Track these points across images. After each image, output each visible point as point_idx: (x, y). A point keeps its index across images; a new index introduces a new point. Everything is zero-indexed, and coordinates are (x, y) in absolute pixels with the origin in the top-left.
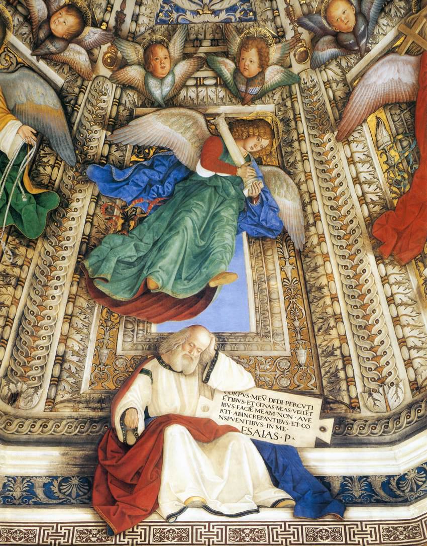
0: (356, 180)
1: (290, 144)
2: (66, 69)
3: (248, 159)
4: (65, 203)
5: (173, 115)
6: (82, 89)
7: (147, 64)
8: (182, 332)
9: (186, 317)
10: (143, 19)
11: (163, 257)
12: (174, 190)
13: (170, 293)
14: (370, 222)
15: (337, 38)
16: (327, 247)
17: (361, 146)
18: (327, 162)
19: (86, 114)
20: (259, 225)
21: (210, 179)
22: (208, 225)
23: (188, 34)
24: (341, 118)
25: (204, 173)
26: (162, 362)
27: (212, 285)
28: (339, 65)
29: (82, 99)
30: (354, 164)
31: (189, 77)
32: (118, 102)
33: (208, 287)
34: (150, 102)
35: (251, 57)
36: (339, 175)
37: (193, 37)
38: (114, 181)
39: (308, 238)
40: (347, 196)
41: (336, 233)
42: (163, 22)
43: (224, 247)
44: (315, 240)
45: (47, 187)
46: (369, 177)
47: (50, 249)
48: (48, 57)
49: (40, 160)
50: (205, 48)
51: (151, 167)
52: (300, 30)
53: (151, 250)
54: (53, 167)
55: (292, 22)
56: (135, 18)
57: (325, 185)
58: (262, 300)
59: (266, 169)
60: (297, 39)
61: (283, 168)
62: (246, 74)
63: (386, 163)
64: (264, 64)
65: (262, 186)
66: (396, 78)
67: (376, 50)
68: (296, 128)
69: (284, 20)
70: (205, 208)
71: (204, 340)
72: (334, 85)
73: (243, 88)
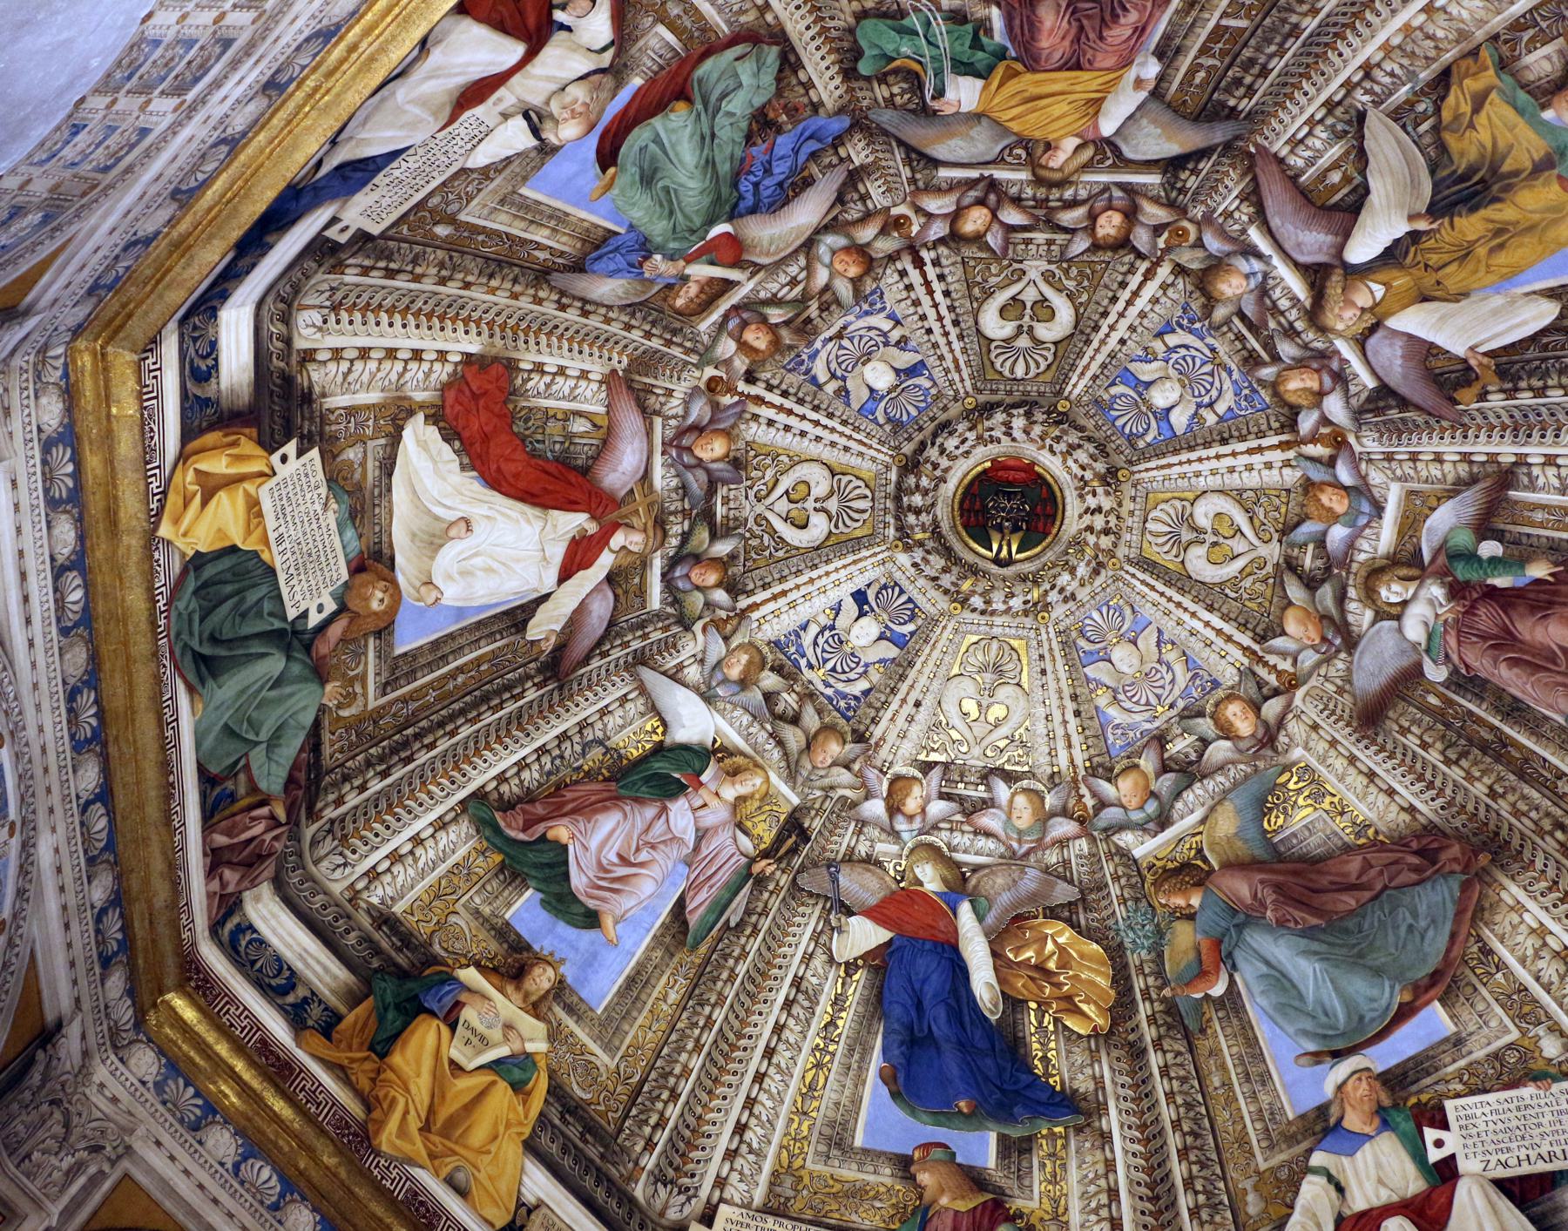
0: (561, 371)
1: (653, 324)
2: (944, 186)
3: (685, 279)
4: (849, 73)
5: (797, 238)
8: (602, 111)
9: (612, 122)
11: (692, 136)
12: (737, 190)
13: (652, 121)
14: (511, 366)
16: (525, 303)
17: (589, 394)
18: (601, 348)
19: (891, 163)
20: (617, 249)
21: (707, 232)
22: (670, 202)
24: (630, 388)
26: (595, 72)
27: (612, 170)
28: (674, 417)
29: (906, 172)
30: (578, 378)
31: (808, 277)
32: (864, 198)
33: (614, 164)
35: (757, 338)
36: (580, 352)
37: (833, 307)
38: (811, 137)
39: (552, 288)
40: (555, 351)
41: (529, 318)
42: (872, 294)
43: (634, 204)
44: (542, 294)
45: (886, 74)
46: (555, 388)
47: (831, 24)
48: (971, 184)
49: (914, 93)
50: (813, 310)
51: (780, 184)
52: (736, 398)
53: (712, 128)
54: (892, 95)
55: (748, 396)
56: (903, 274)
57: (583, 332)
58: (541, 213)
59: (656, 288)
60: (732, 390)
61: (641, 303)
62: (753, 327)
63: (554, 416)
64: (743, 346)
65: (647, 275)
66: (621, 469)
67: (658, 460)
68: (660, 337)
70: (688, 210)
71: (568, 131)
72: (662, 399)
73: (745, 315)
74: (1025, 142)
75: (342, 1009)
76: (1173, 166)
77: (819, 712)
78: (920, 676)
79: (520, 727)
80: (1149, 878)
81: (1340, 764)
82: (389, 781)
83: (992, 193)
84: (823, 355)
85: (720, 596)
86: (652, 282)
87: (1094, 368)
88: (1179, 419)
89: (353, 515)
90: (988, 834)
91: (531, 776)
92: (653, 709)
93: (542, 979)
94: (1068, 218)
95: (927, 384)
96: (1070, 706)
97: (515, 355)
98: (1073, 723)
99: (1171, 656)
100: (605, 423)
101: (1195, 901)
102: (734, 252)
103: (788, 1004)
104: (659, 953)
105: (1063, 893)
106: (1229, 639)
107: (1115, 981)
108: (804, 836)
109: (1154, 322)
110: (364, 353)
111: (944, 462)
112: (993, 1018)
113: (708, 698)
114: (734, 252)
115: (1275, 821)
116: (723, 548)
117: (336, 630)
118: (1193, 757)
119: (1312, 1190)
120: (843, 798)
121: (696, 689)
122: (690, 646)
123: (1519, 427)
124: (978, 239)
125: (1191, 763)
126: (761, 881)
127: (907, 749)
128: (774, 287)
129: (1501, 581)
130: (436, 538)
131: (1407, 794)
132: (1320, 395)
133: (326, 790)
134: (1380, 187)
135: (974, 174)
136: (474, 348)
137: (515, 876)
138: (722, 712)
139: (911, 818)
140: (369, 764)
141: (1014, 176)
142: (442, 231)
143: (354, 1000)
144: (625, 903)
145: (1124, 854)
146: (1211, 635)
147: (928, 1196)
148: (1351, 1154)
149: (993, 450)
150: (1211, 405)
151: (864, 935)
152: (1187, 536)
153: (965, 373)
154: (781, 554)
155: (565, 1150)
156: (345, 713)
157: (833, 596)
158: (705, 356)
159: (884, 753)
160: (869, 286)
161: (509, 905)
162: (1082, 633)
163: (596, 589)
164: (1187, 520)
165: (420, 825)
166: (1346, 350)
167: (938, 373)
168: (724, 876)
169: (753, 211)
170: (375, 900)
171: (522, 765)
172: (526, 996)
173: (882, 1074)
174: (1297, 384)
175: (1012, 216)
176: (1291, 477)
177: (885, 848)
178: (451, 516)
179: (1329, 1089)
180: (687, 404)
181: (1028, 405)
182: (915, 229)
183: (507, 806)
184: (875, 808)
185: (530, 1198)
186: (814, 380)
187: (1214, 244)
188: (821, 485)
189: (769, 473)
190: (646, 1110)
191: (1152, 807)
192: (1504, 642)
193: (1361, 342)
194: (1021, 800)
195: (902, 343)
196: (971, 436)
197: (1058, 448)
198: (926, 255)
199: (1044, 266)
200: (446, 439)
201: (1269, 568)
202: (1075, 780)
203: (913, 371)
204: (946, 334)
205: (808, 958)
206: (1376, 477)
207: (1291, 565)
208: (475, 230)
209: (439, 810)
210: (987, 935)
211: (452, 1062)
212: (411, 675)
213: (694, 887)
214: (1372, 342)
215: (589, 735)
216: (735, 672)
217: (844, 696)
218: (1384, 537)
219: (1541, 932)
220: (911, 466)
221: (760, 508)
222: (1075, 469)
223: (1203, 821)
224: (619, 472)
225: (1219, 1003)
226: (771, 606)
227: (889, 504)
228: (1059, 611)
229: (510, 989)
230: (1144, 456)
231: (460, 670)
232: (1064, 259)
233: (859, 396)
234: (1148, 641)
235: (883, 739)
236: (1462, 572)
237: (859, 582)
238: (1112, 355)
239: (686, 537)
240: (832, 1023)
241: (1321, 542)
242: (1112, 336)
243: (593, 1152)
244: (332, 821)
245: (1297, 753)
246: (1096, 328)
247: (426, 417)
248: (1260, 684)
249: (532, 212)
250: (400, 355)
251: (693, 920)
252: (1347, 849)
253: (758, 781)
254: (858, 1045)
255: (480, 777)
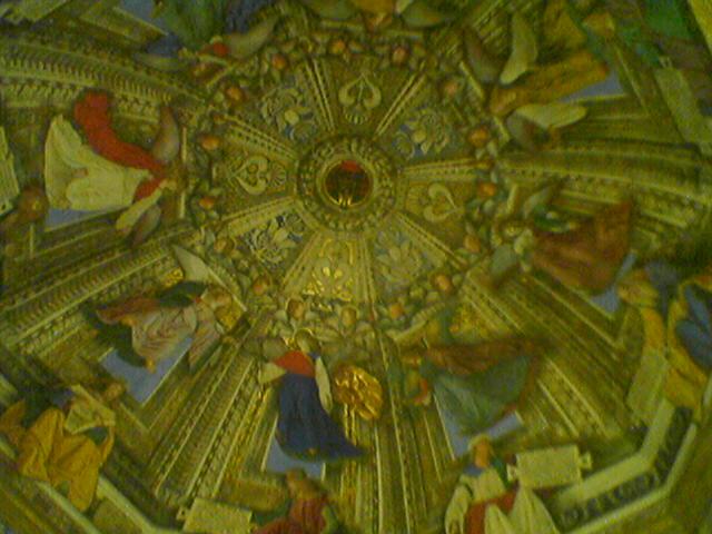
1: (184, 82)
3: (198, 61)
6: (309, 24)
7: (285, 58)
10: (299, 71)
14: (110, 96)
15: (205, 135)
16: (117, 65)
23: (274, 82)
25: (216, 39)
29: (306, 22)
32: (287, 31)
34: (270, 43)
35: (236, 96)
48: (336, 30)
60: (222, 117)
64: (227, 97)
67: (184, 147)
69: (235, 119)
74: (363, 13)
75: (7, 404)
76: (428, 30)
77: (259, 270)
78: (307, 254)
79: (112, 270)
80: (399, 350)
81: (483, 305)
82: (41, 293)
83: (346, 36)
84: (265, 105)
85: (214, 214)
86: (183, 61)
87: (390, 121)
88: (425, 149)
89: (23, 161)
90: (331, 328)
91: (116, 294)
92: (179, 264)
93: (115, 391)
94: (382, 50)
95: (313, 123)
96: (370, 273)
97: (112, 90)
98: (371, 281)
99: (415, 253)
100: (158, 127)
101: (419, 361)
102: (224, 51)
103: (235, 403)
104: (174, 379)
105: (363, 355)
106: (440, 248)
107: (383, 397)
108: (249, 326)
109: (417, 102)
110: (30, 82)
111: (320, 160)
112: (328, 412)
113: (206, 261)
114: (224, 51)
115: (454, 329)
116: (216, 192)
117: (13, 218)
118: (421, 297)
119: (460, 493)
120: (267, 309)
121: (200, 256)
122: (198, 237)
123: (569, 162)
124: (339, 57)
125: (420, 301)
126: (226, 346)
127: (297, 288)
128: (242, 70)
129: (556, 230)
130: (68, 176)
131: (511, 319)
132: (485, 143)
133: (5, 298)
134: (517, 51)
135: (338, 25)
136: (90, 84)
137: (104, 341)
138: (212, 268)
139: (297, 319)
140: (29, 284)
141: (356, 28)
142: (71, 24)
143: (14, 400)
144: (160, 355)
145: (390, 340)
146: (432, 245)
147: (292, 493)
148: (476, 477)
149: (341, 156)
150: (439, 143)
151: (273, 372)
152: (424, 201)
153: (331, 120)
154: (243, 197)
155: (120, 472)
156: (16, 259)
157: (267, 217)
158: (210, 100)
159: (287, 290)
160: (288, 73)
161: (101, 354)
162: (377, 241)
163: (153, 207)
164: (425, 194)
165: (57, 315)
166: (498, 123)
167: (319, 119)
168: (209, 343)
169: (234, 30)
170: (29, 351)
171: (111, 289)
172: (105, 399)
173: (276, 436)
174: (477, 136)
175: (355, 47)
176: (471, 178)
177: (284, 332)
178: (77, 166)
179: (470, 447)
180: (200, 122)
181: (359, 137)
182: (310, 48)
183: (101, 307)
184: (282, 314)
185: (100, 494)
186: (261, 116)
187: (444, 68)
188: (263, 166)
189: (239, 158)
190: (163, 454)
191: (402, 319)
192: (555, 257)
193: (505, 119)
194: (347, 314)
195: (303, 103)
196: (333, 150)
197: (372, 158)
198: (315, 63)
199: (368, 72)
200: (74, 127)
201: (459, 217)
202: (371, 306)
203: (309, 116)
204: (323, 101)
205: (246, 383)
206: (507, 181)
207: (468, 217)
208: (89, 26)
209: (66, 309)
210: (328, 372)
211: (65, 432)
212: (53, 243)
213: (193, 348)
214: (510, 120)
215: (146, 275)
216: (219, 249)
217: (269, 262)
218: (509, 207)
219: (561, 382)
220: (305, 161)
221: (234, 175)
222: (378, 167)
223: (424, 327)
224: (167, 150)
225: (426, 408)
226: (237, 221)
227: (294, 178)
228: (368, 231)
229: (98, 395)
230: (409, 164)
231: (80, 241)
232: (378, 69)
233: (282, 126)
234: (405, 247)
235: (287, 282)
236: (538, 224)
237: (280, 212)
238: (397, 116)
239: (197, 186)
240: (255, 412)
241: (481, 207)
242: (399, 107)
243: (135, 475)
244: (8, 313)
245: (466, 299)
246: (391, 103)
247: (64, 117)
248: (452, 268)
249: (121, 21)
250: (50, 84)
251: (192, 364)
252: (484, 342)
253: (228, 300)
254: (267, 423)
255: (91, 292)
